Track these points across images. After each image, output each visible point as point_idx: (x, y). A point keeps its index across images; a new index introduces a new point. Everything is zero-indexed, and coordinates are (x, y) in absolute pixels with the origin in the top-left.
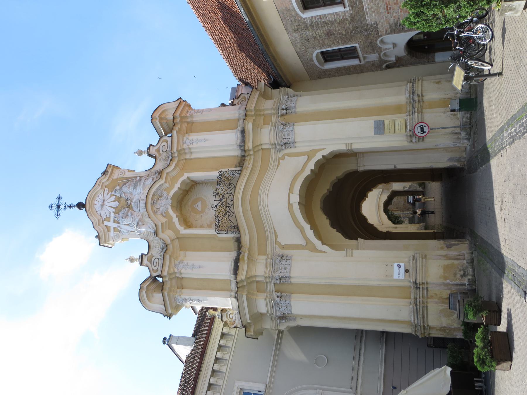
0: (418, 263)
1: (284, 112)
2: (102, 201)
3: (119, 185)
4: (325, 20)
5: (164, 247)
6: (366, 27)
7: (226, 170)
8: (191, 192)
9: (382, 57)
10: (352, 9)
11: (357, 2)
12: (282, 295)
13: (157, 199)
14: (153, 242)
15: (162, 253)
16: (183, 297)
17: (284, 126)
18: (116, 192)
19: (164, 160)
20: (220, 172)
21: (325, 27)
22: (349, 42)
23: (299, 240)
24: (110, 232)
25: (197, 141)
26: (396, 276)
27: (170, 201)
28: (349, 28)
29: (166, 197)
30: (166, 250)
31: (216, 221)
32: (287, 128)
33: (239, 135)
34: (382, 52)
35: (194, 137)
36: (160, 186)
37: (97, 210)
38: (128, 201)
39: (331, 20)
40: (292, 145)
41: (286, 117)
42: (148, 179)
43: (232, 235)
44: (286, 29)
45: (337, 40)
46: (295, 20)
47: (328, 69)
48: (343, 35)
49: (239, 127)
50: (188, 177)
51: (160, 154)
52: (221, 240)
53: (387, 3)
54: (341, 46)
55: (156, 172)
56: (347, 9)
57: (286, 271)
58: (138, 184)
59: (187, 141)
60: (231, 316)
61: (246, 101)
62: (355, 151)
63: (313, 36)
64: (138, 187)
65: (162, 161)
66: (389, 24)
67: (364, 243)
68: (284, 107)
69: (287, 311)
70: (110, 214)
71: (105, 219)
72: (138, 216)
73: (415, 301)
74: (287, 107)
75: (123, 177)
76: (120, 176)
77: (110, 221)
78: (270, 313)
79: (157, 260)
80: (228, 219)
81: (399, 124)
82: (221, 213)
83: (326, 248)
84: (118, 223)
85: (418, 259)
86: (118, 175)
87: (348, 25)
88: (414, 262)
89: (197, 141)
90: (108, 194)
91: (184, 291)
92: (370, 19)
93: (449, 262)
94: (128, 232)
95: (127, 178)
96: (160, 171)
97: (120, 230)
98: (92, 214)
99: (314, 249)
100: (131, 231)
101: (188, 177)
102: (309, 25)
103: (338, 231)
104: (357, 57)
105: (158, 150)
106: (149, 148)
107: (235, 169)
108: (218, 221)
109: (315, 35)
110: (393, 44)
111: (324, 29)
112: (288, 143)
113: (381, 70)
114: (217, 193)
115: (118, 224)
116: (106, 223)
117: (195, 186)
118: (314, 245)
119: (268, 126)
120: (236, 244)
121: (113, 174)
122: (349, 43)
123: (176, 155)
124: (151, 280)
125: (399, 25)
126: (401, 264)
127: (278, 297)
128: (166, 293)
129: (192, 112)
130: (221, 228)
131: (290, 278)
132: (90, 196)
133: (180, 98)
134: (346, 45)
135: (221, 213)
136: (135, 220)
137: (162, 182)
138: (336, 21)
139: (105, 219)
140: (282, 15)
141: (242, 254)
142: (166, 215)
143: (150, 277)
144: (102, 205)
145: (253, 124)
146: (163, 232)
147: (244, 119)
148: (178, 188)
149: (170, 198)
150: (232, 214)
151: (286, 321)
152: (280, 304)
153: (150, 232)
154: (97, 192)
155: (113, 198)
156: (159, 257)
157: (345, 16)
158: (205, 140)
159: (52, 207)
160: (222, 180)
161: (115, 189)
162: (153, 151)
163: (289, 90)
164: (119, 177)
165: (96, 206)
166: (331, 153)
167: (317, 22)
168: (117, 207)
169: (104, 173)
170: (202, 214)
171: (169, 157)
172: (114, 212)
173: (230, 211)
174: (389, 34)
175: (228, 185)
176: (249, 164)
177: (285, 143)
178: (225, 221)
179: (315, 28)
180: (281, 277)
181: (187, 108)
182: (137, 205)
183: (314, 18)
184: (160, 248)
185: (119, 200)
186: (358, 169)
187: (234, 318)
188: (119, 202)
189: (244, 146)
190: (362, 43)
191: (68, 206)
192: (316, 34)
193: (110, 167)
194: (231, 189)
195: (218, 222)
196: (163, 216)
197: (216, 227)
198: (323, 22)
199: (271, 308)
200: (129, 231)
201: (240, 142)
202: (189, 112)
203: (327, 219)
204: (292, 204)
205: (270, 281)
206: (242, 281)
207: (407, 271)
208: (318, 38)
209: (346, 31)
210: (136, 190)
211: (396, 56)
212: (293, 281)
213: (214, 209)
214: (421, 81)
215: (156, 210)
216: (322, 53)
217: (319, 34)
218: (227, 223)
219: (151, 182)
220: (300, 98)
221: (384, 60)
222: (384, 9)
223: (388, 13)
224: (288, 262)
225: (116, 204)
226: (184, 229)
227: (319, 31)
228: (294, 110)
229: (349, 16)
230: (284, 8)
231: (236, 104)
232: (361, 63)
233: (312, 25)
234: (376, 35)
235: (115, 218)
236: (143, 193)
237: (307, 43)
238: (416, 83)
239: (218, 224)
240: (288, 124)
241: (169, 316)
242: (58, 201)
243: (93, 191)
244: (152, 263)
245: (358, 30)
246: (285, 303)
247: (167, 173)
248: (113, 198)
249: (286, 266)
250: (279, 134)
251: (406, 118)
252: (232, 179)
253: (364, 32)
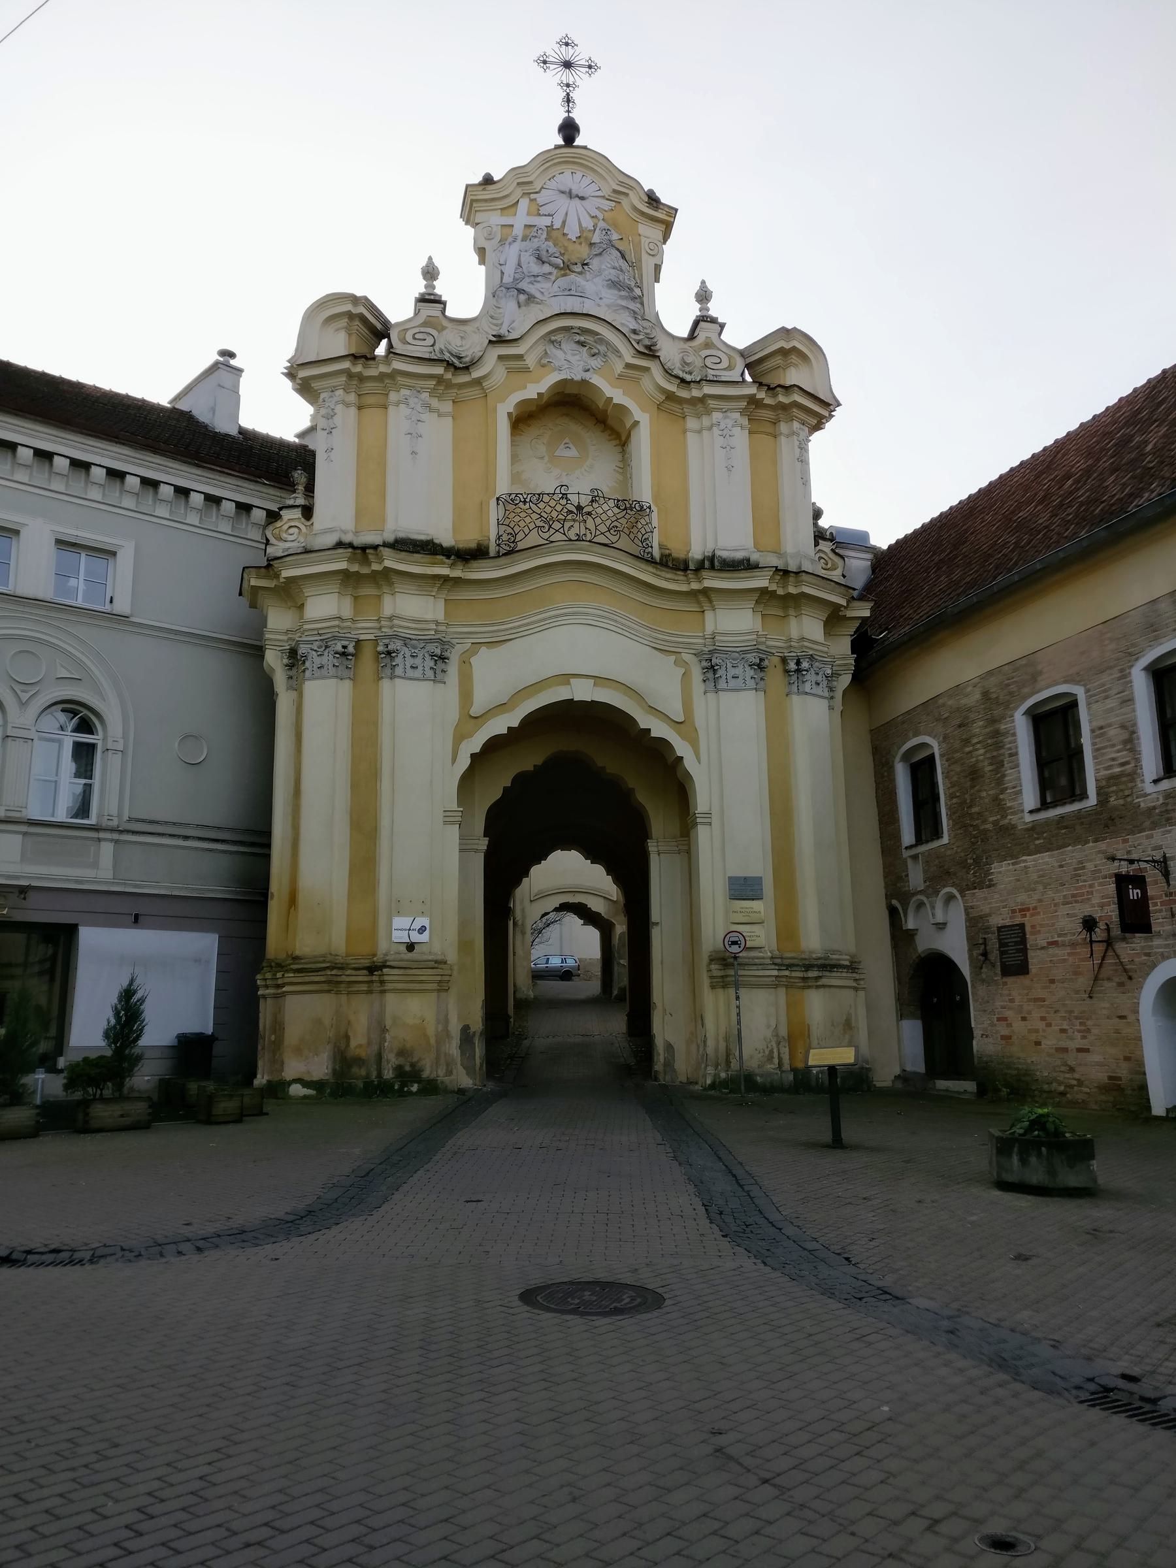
0: (430, 972)
1: (792, 666)
2: (580, 195)
3: (622, 239)
4: (1006, 765)
5: (464, 360)
6: (984, 860)
7: (655, 523)
8: (603, 432)
9: (914, 899)
10: (1027, 830)
11: (1042, 841)
12: (350, 657)
13: (584, 342)
14: (475, 332)
15: (449, 355)
16: (339, 408)
17: (759, 665)
18: (604, 232)
19: (685, 363)
20: (650, 508)
21: (991, 764)
22: (953, 821)
23: (481, 700)
24: (501, 215)
25: (728, 448)
26: (400, 922)
27: (577, 378)
28: (985, 822)
29: (589, 367)
30: (456, 368)
31: (530, 496)
32: (752, 673)
33: (739, 555)
34: (928, 898)
35: (741, 438)
36: (618, 352)
37: (559, 178)
38: (579, 265)
39: (1007, 778)
40: (711, 684)
41: (780, 668)
42: (636, 318)
43: (493, 537)
44: (990, 673)
45: (958, 794)
46: (1011, 694)
47: (894, 771)
48: (970, 807)
49: (758, 553)
50: (636, 423)
51: (697, 351)
52: (482, 508)
53: (1035, 908)
54: (946, 803)
55: (655, 340)
56: (1028, 818)
57: (408, 667)
58: (623, 293)
59: (730, 423)
60: (292, 530)
61: (822, 573)
62: (692, 833)
63: (971, 737)
64: (616, 292)
65: (682, 355)
66: (989, 915)
67: (477, 851)
68: (805, 665)
69: (310, 669)
70: (546, 215)
71: (535, 199)
72: (542, 293)
73: (340, 965)
74: (804, 673)
75: (643, 251)
76: (644, 242)
77: (528, 214)
78: (306, 627)
79: (430, 341)
80: (532, 526)
81: (753, 934)
82: (548, 509)
83: (464, 762)
84: (524, 239)
85: (439, 971)
86: (648, 238)
87: (991, 819)
88: (432, 964)
89: (728, 448)
90: (598, 208)
91: (353, 411)
92: (1002, 871)
93: (432, 1041)
94: (501, 265)
95: (641, 261)
96: (657, 351)
97: (507, 243)
98: (548, 164)
99: (460, 737)
100: (502, 273)
101: (636, 423)
102: (998, 726)
103: (505, 789)
104: (919, 841)
105: (708, 345)
106: (713, 321)
107: (655, 545)
108: (528, 500)
109: (975, 740)
110: (945, 924)
111: (986, 763)
112: (714, 674)
113: (886, 895)
114: (597, 498)
115: (520, 238)
116: (524, 204)
117: (617, 442)
118: (470, 735)
119: (758, 626)
120: (473, 545)
121: (650, 223)
122: (951, 821)
123: (696, 393)
124: (379, 326)
125: (986, 936)
126: (427, 933)
127: (344, 647)
128: (346, 365)
129: (803, 434)
130: (511, 507)
131: (392, 677)
132: (593, 159)
133: (839, 405)
134: (947, 815)
135: (548, 509)
136: (531, 283)
137: (629, 357)
138: (1003, 791)
139: (535, 199)
140: (1024, 662)
141: (447, 561)
142: (544, 364)
143: (386, 323)
144: (570, 195)
145: (763, 591)
146: (500, 357)
147: (776, 567)
149: (587, 376)
150: (546, 536)
151: (286, 666)
152: (326, 653)
153: (502, 324)
154: (605, 179)
155: (588, 223)
156: (437, 348)
157: (1013, 813)
158: (729, 469)
159: (567, 44)
160: (629, 511)
161: (613, 231)
162: (705, 331)
163: (846, 680)
164: (643, 239)
165: (568, 174)
166: (688, 775)
167: (1002, 747)
168: (564, 234)
169: (652, 199)
170: (546, 458)
171: (690, 373)
172: (552, 225)
173: (552, 531)
174: (967, 914)
175: (617, 527)
176: (666, 579)
177: (715, 668)
178: (528, 520)
179: (989, 741)
180: (393, 655)
181: (814, 422)
182: (570, 290)
183: (1013, 738)
184: (460, 349)
185: (582, 240)
186: (651, 839)
187: (290, 538)
188: (579, 241)
189: (712, 567)
190: (949, 853)
191: (568, 94)
192: (978, 743)
193: (669, 214)
194: (607, 534)
195: (525, 502)
196: (541, 359)
197: (513, 496)
198: (1003, 761)
199: (318, 629)
200: (503, 267)
201: (721, 557)
202: (802, 426)
203: (535, 766)
204: (569, 683)
205: (383, 630)
206: (381, 560)
207: (411, 947)
208: (967, 749)
209: (979, 813)
210: (609, 287)
211: (917, 930)
212: (386, 684)
213: (558, 491)
214: (854, 984)
215: (556, 340)
216: (932, 758)
217: (977, 750)
218: (522, 524)
219: (627, 326)
220: (824, 704)
221: (909, 904)
222: (1022, 904)
223: (1014, 911)
224: (430, 674)
225: (573, 231)
226: (509, 414)
227: (981, 751)
228: (796, 690)
229: (1013, 823)
230: (1039, 667)
231: (818, 548)
232: (904, 851)
233: (996, 734)
234: (965, 884)
235: (536, 228)
236: (599, 306)
237: (957, 722)
238: (849, 975)
239: (520, 501)
240: (762, 675)
241: (291, 374)
242: (583, 62)
243: (605, 167)
244: (422, 330)
245: (979, 843)
246: (330, 667)
248: (588, 223)
249: (420, 668)
250: (737, 654)
251: (766, 949)
252: (632, 536)
253: (974, 856)
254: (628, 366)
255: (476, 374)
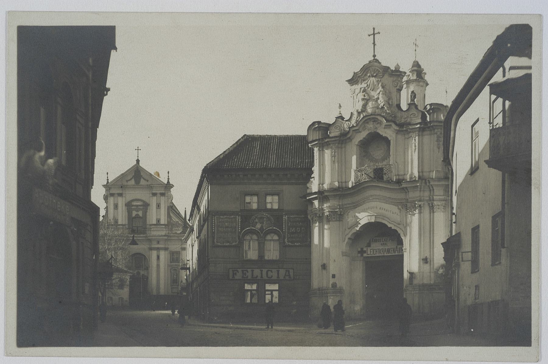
148: (382, 135)
224: (338, 219)
247: (391, 125)
249: (336, 218)
254: (385, 125)
255: (349, 136)
